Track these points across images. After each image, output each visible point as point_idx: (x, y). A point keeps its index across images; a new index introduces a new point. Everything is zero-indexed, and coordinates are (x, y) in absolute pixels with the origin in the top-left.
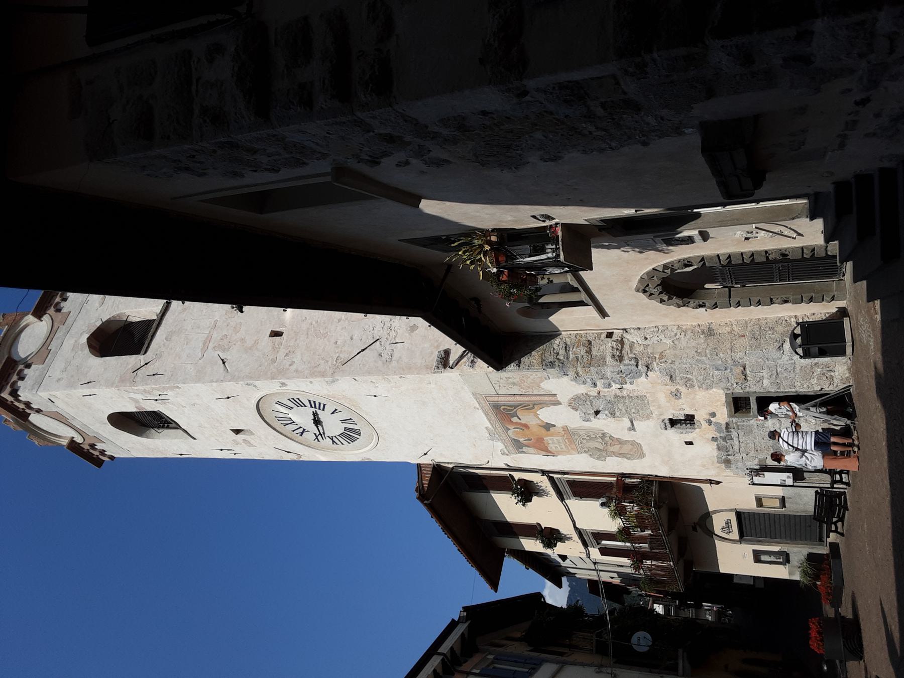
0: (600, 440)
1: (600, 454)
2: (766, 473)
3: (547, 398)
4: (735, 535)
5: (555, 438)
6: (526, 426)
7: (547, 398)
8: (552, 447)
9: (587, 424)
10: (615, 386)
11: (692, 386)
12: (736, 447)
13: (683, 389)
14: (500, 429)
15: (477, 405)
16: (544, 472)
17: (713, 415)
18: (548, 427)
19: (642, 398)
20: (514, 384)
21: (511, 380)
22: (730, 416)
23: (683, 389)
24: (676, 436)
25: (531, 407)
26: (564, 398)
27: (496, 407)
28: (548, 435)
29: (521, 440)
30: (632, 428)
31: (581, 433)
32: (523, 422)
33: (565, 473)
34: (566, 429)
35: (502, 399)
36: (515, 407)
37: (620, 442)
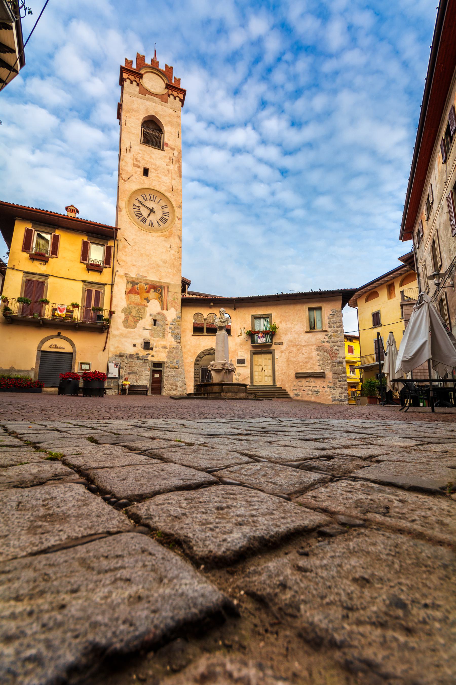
1: (127, 312)
2: (118, 368)
3: (165, 307)
4: (46, 347)
6: (148, 292)
7: (165, 307)
8: (132, 296)
9: (148, 314)
10: (170, 331)
11: (168, 353)
12: (132, 360)
13: (167, 350)
14: (146, 281)
15: (162, 281)
16: (112, 285)
17: (153, 356)
18: (148, 301)
19: (163, 337)
20: (174, 299)
21: (176, 300)
22: (152, 362)
23: (167, 350)
24: (139, 342)
25: (161, 298)
26: (164, 312)
27: (161, 287)
28: (141, 298)
29: (138, 286)
30: (144, 329)
31: (142, 310)
32: (151, 292)
34: (147, 306)
35: (166, 292)
37: (136, 322)
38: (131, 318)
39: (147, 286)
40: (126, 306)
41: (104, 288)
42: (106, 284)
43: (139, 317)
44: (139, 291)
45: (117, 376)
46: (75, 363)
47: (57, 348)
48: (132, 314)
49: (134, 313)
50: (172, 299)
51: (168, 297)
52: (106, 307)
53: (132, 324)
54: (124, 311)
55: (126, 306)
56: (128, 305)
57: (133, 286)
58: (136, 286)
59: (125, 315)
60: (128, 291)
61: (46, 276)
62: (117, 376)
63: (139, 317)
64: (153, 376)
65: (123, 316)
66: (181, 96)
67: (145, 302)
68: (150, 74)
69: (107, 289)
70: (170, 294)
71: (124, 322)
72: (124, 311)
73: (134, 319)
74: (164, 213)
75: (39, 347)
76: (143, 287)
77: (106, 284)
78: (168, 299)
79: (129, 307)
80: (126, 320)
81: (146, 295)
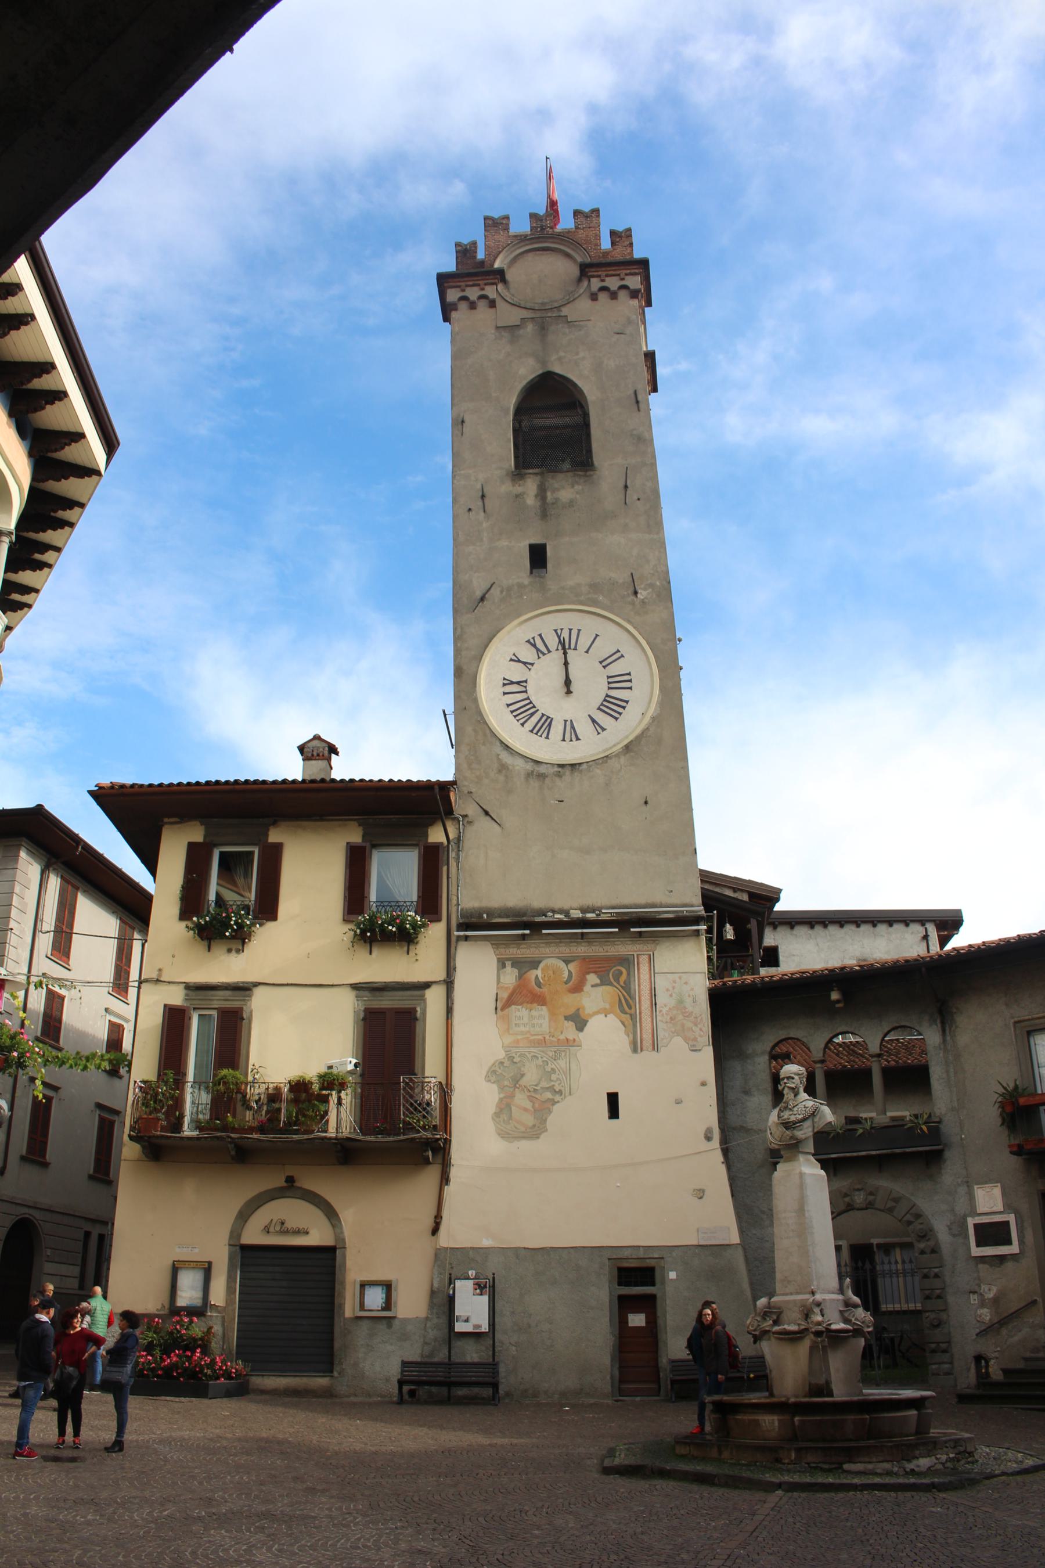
0: (544, 1084)
1: (507, 1075)
2: (485, 1299)
4: (253, 1235)
5: (545, 1023)
6: (578, 988)
7: (647, 1036)
8: (520, 1013)
16: (449, 983)
21: (688, 1002)
28: (553, 1014)
29: (539, 972)
31: (562, 1063)
32: (587, 988)
33: (449, 1010)
36: (627, 988)
37: (542, 1111)
38: (521, 1099)
39: (571, 966)
40: (501, 1055)
41: (422, 998)
42: (427, 985)
43: (551, 1089)
44: (545, 990)
45: (485, 1328)
46: (343, 1283)
47: (286, 1232)
48: (523, 1082)
49: (531, 1075)
50: (672, 1002)
51: (653, 995)
52: (432, 1068)
53: (529, 1120)
54: (494, 1074)
55: (501, 1055)
56: (507, 1049)
57: (520, 976)
58: (533, 974)
59: (502, 1088)
60: (504, 995)
61: (244, 989)
62: (485, 1328)
63: (551, 1089)
64: (623, 1321)
65: (491, 1095)
66: (634, 282)
67: (569, 1030)
68: (530, 257)
69: (434, 998)
70: (661, 983)
71: (497, 1115)
72: (494, 1074)
73: (531, 1098)
74: (612, 682)
75: (235, 1233)
76: (556, 971)
77: (427, 985)
78: (654, 1004)
79: (511, 1058)
80: (504, 1109)
81: (570, 1002)
